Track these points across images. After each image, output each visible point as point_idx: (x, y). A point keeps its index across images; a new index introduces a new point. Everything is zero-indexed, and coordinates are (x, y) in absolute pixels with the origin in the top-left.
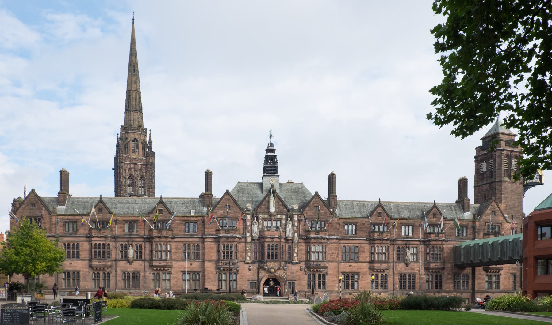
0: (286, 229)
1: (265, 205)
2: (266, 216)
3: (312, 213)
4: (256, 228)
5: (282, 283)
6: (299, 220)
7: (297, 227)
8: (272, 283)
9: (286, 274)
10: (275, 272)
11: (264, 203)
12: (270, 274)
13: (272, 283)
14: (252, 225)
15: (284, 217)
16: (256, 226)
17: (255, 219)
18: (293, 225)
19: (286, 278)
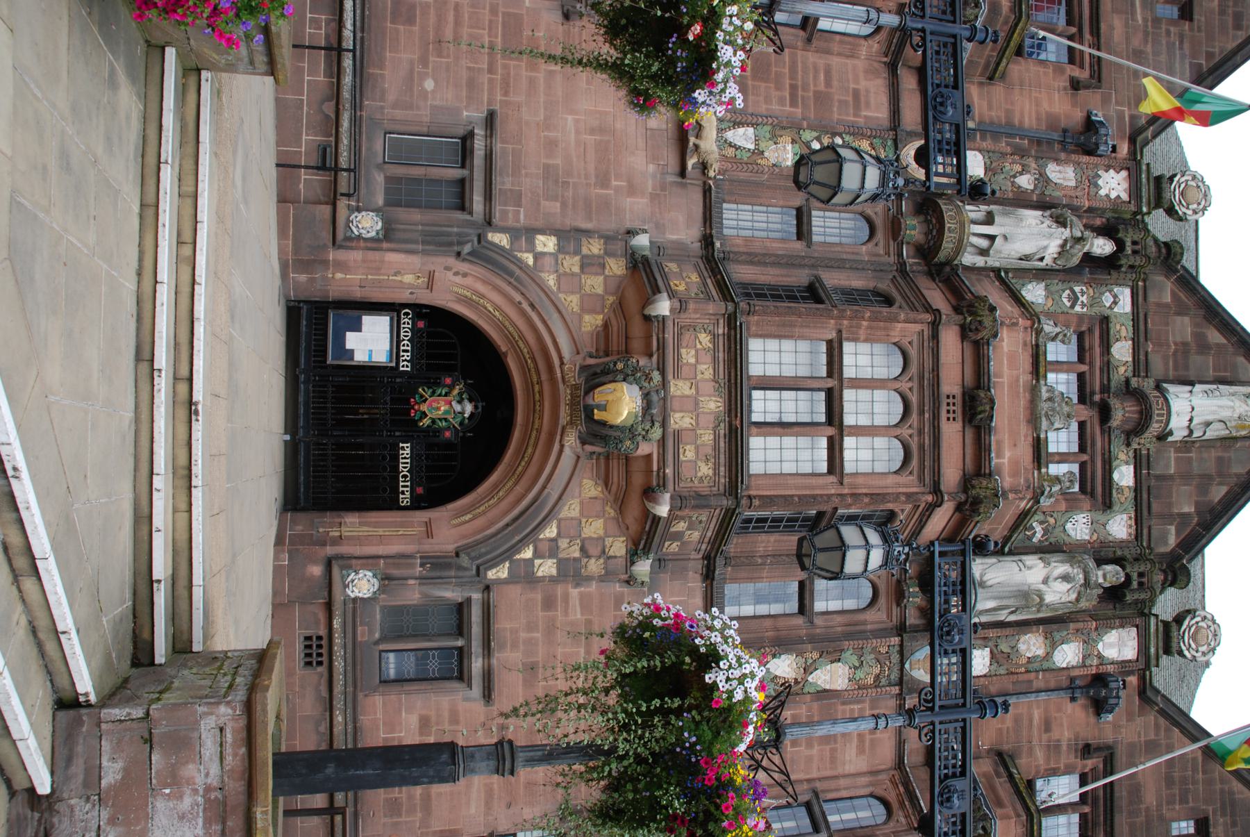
0: (1048, 549)
1: (1203, 347)
2: (1122, 351)
3: (1150, 798)
4: (1029, 237)
5: (450, 526)
6: (1100, 679)
7: (1042, 665)
8: (447, 408)
9: (570, 572)
10: (598, 433)
11: (1215, 336)
12: (574, 378)
13: (447, 408)
14: (1047, 203)
15: (1119, 527)
16: (1053, 248)
17: (1102, 246)
18: (1055, 623)
19: (524, 576)
